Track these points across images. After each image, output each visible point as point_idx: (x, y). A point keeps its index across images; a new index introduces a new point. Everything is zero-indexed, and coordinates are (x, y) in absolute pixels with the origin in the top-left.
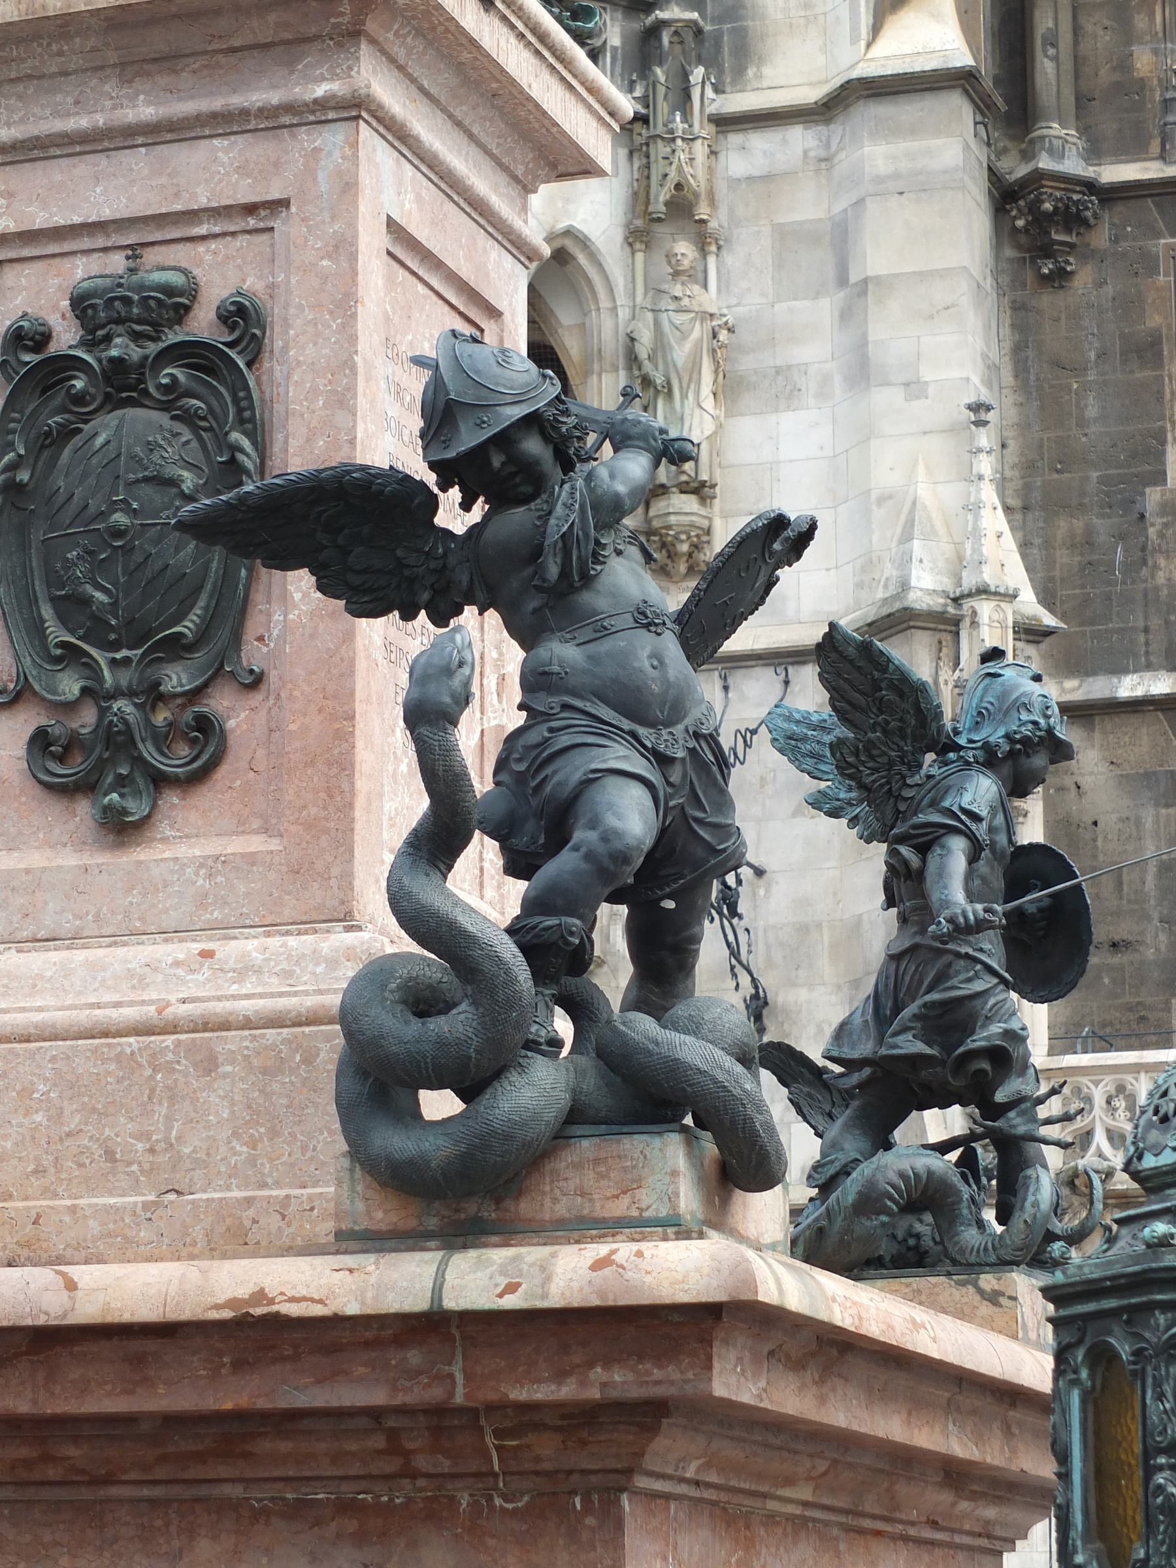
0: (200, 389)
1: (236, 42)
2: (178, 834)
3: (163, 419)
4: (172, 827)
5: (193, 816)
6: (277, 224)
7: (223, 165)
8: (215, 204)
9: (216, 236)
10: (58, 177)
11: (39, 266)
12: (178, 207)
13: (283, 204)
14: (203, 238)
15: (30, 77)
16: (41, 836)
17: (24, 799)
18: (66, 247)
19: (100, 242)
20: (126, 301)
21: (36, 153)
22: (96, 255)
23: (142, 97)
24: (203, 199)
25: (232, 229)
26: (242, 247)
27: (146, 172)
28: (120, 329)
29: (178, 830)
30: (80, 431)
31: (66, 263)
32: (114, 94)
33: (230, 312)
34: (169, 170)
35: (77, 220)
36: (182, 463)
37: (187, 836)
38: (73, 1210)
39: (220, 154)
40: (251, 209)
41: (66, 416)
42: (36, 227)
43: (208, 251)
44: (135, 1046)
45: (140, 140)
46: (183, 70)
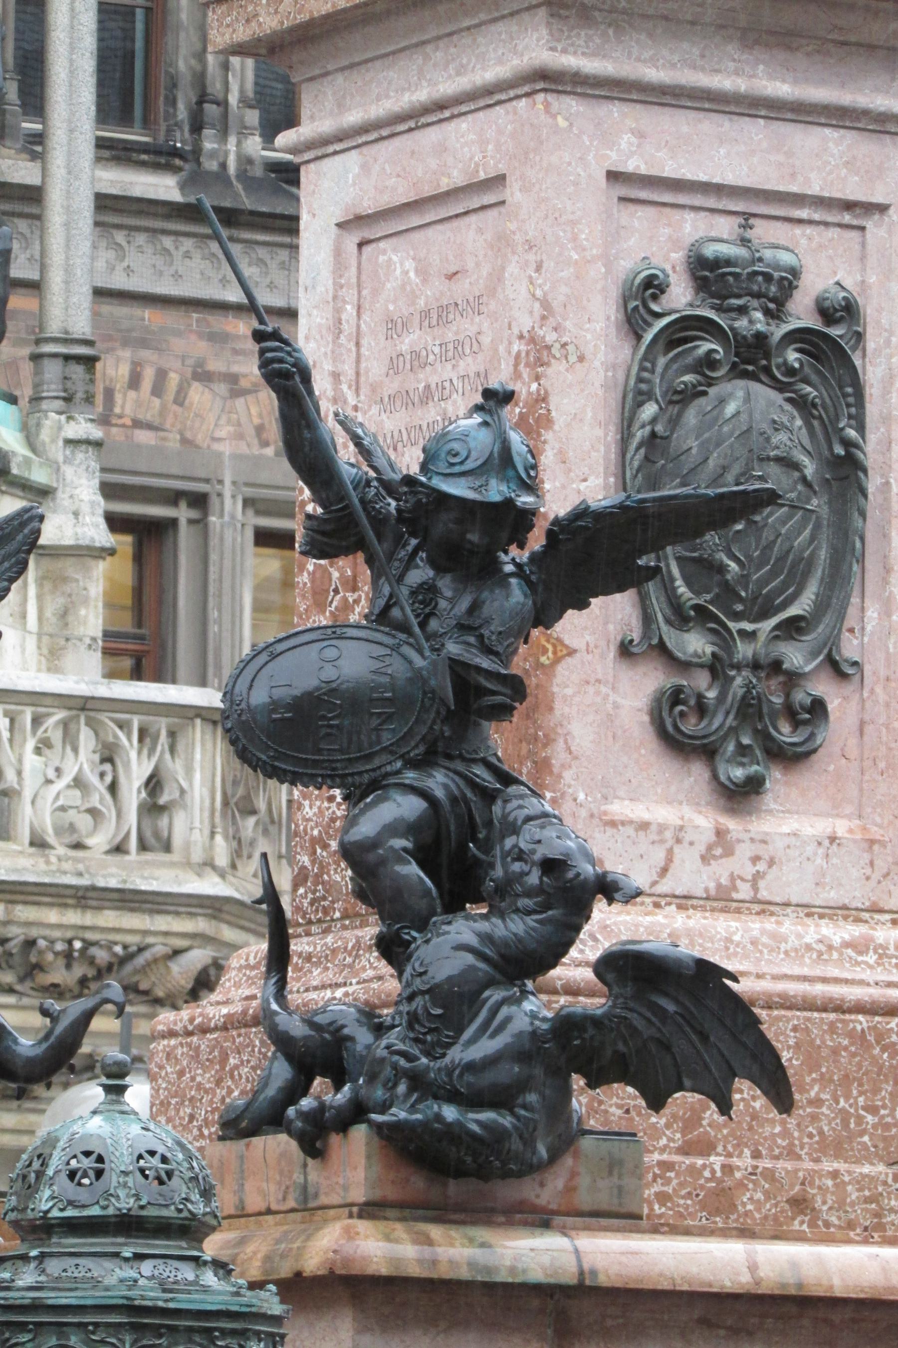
0: (814, 378)
1: (853, 39)
2: (781, 808)
3: (777, 397)
4: (775, 801)
5: (794, 793)
6: (869, 224)
7: (832, 155)
8: (826, 194)
9: (810, 222)
10: (685, 129)
11: (651, 211)
12: (794, 189)
13: (882, 208)
14: (800, 221)
15: (666, 18)
16: (659, 791)
17: (643, 751)
18: (682, 199)
19: (711, 202)
20: (768, 277)
21: (668, 99)
22: (703, 214)
23: (761, 67)
24: (815, 188)
25: (830, 219)
26: (833, 239)
27: (765, 145)
28: (755, 303)
29: (781, 805)
30: (704, 393)
31: (676, 214)
32: (736, 57)
33: (840, 305)
34: (786, 148)
35: (703, 177)
36: (799, 448)
37: (789, 812)
38: (835, 1174)
39: (831, 144)
40: (849, 206)
41: (699, 377)
42: (665, 175)
43: (803, 235)
44: (865, 1025)
45: (763, 113)
46: (797, 49)
